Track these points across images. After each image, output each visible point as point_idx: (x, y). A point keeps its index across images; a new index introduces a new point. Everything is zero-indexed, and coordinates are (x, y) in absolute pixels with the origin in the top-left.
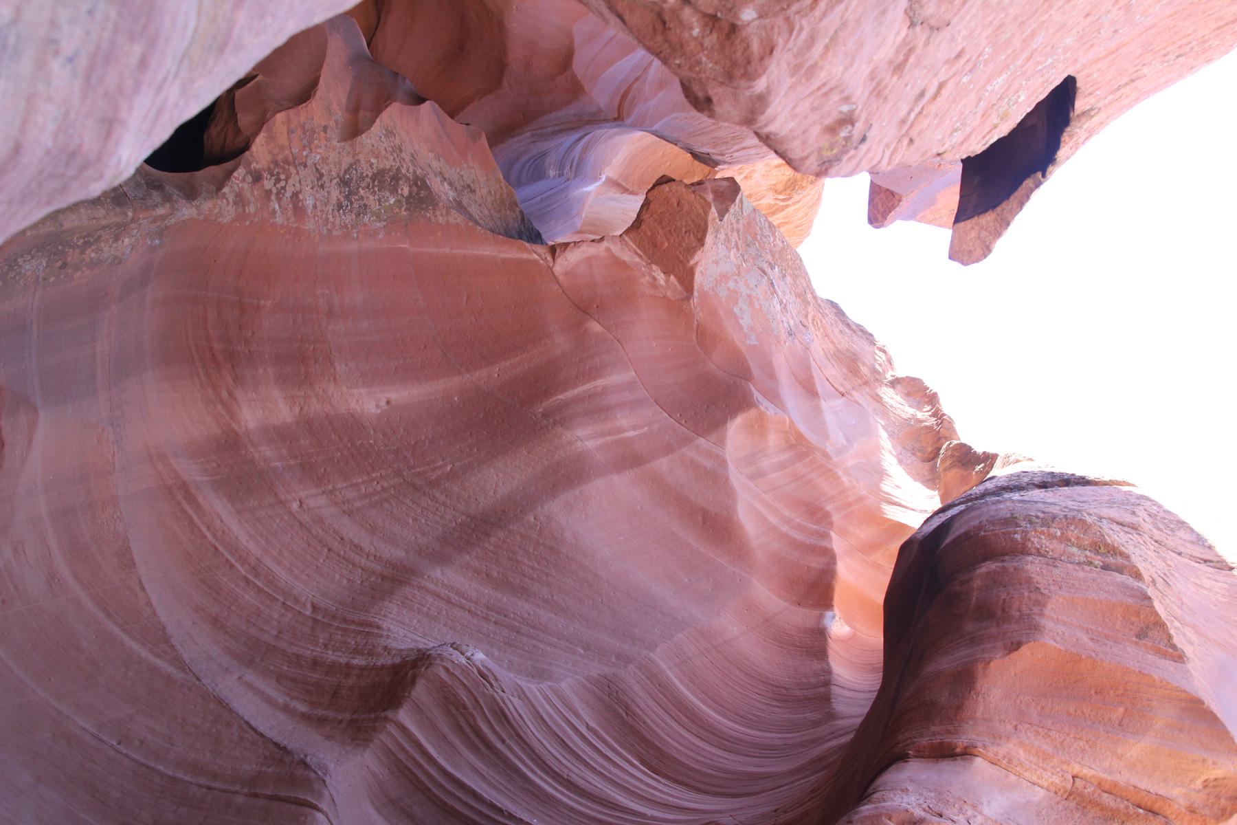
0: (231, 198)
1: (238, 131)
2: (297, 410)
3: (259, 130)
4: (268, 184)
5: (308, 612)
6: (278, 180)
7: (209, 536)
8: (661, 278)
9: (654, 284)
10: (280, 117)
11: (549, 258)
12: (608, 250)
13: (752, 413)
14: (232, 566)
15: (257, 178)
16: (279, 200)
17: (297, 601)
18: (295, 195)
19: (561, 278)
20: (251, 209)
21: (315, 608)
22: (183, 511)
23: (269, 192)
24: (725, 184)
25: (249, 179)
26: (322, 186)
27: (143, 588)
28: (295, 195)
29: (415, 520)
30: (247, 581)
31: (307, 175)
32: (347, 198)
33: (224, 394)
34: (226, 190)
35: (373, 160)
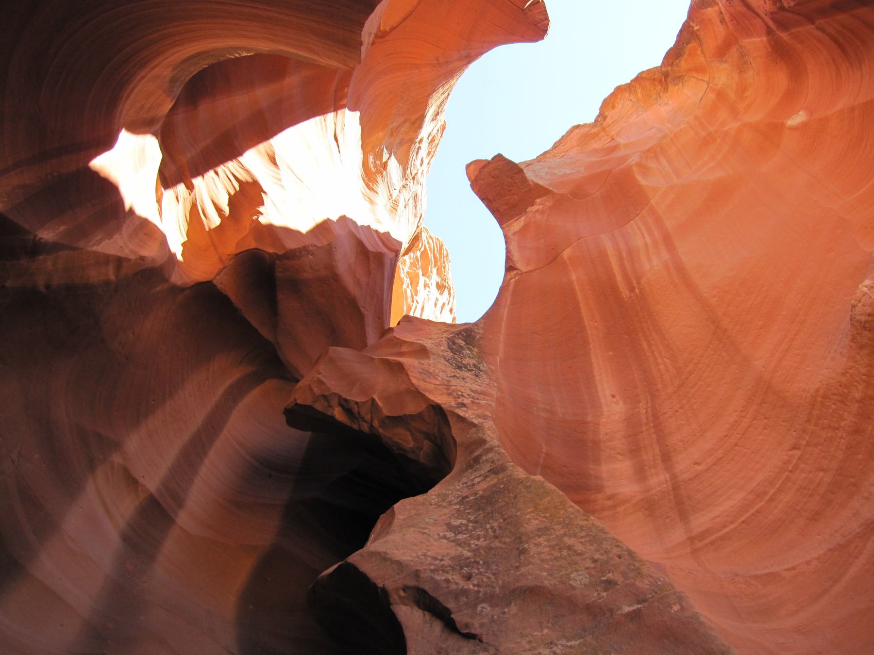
0: (480, 420)
1: (420, 416)
2: (620, 457)
3: (424, 396)
4: (467, 401)
5: (797, 453)
6: (463, 396)
7: (733, 526)
8: (535, 208)
9: (542, 212)
10: (414, 381)
11: (515, 272)
12: (514, 234)
13: (635, 169)
14: (758, 511)
15: (464, 405)
16: (477, 399)
17: (788, 462)
18: (472, 391)
19: (530, 268)
20: (489, 414)
21: (795, 447)
22: (712, 543)
23: (473, 402)
24: (472, 168)
25: (465, 409)
26: (464, 378)
27: (794, 568)
28: (472, 391)
29: (708, 386)
30: (771, 500)
31: (454, 382)
32: (470, 370)
33: (609, 503)
34: (476, 421)
35: (442, 348)
